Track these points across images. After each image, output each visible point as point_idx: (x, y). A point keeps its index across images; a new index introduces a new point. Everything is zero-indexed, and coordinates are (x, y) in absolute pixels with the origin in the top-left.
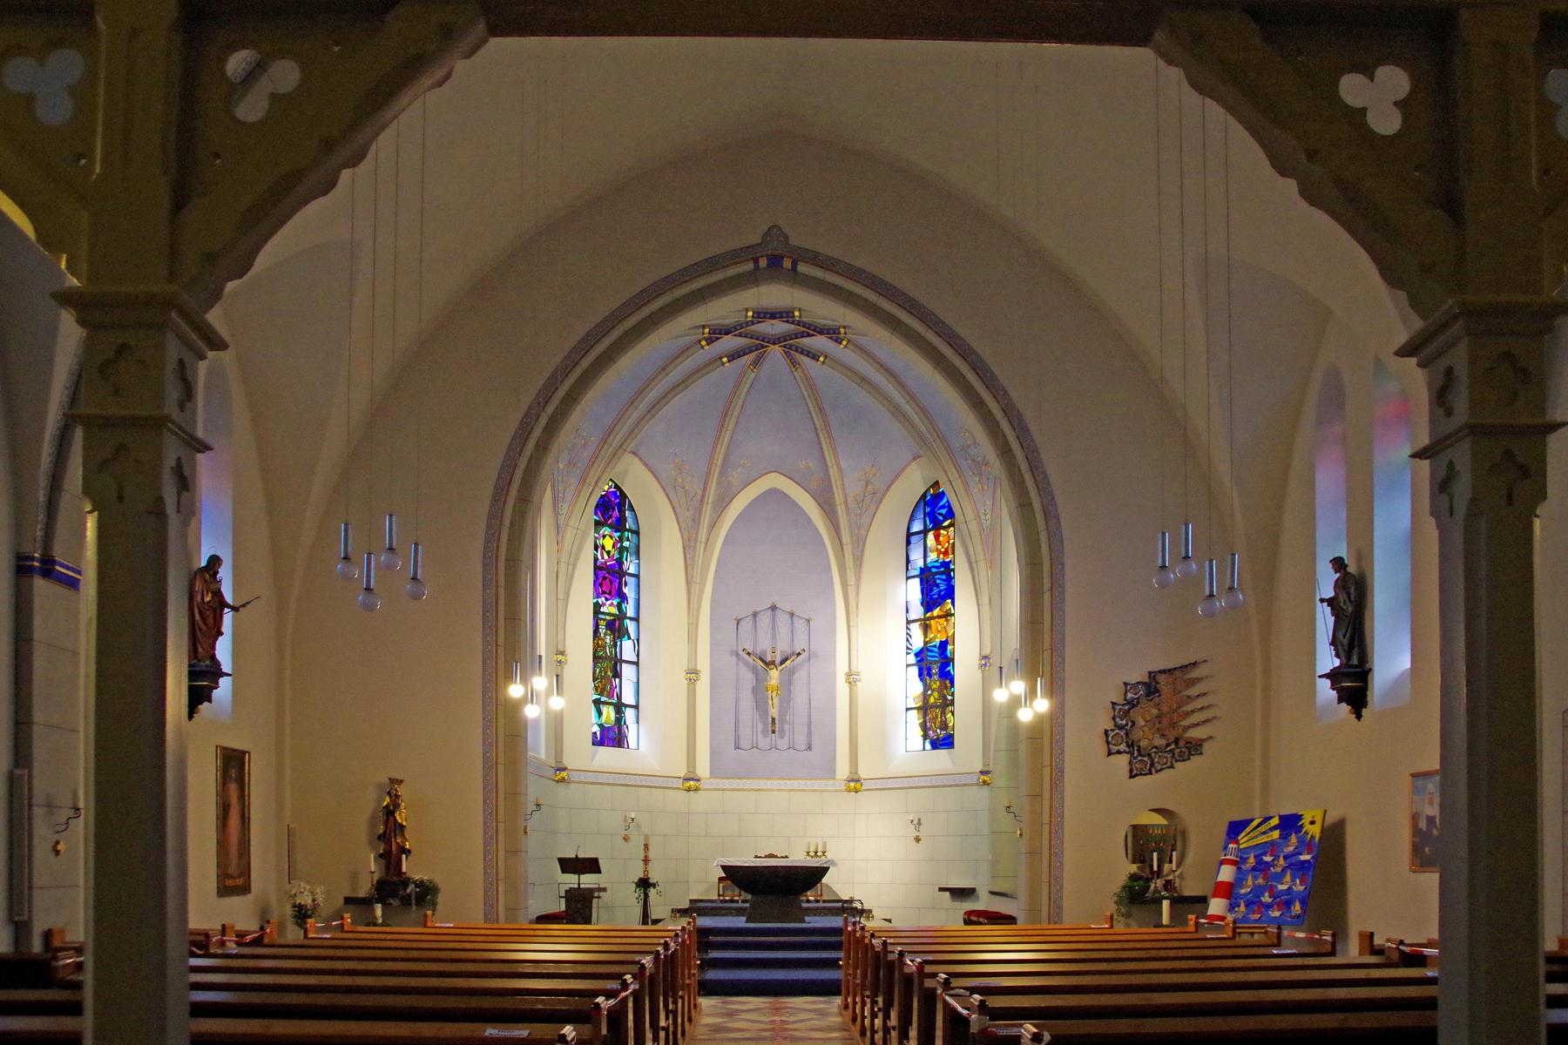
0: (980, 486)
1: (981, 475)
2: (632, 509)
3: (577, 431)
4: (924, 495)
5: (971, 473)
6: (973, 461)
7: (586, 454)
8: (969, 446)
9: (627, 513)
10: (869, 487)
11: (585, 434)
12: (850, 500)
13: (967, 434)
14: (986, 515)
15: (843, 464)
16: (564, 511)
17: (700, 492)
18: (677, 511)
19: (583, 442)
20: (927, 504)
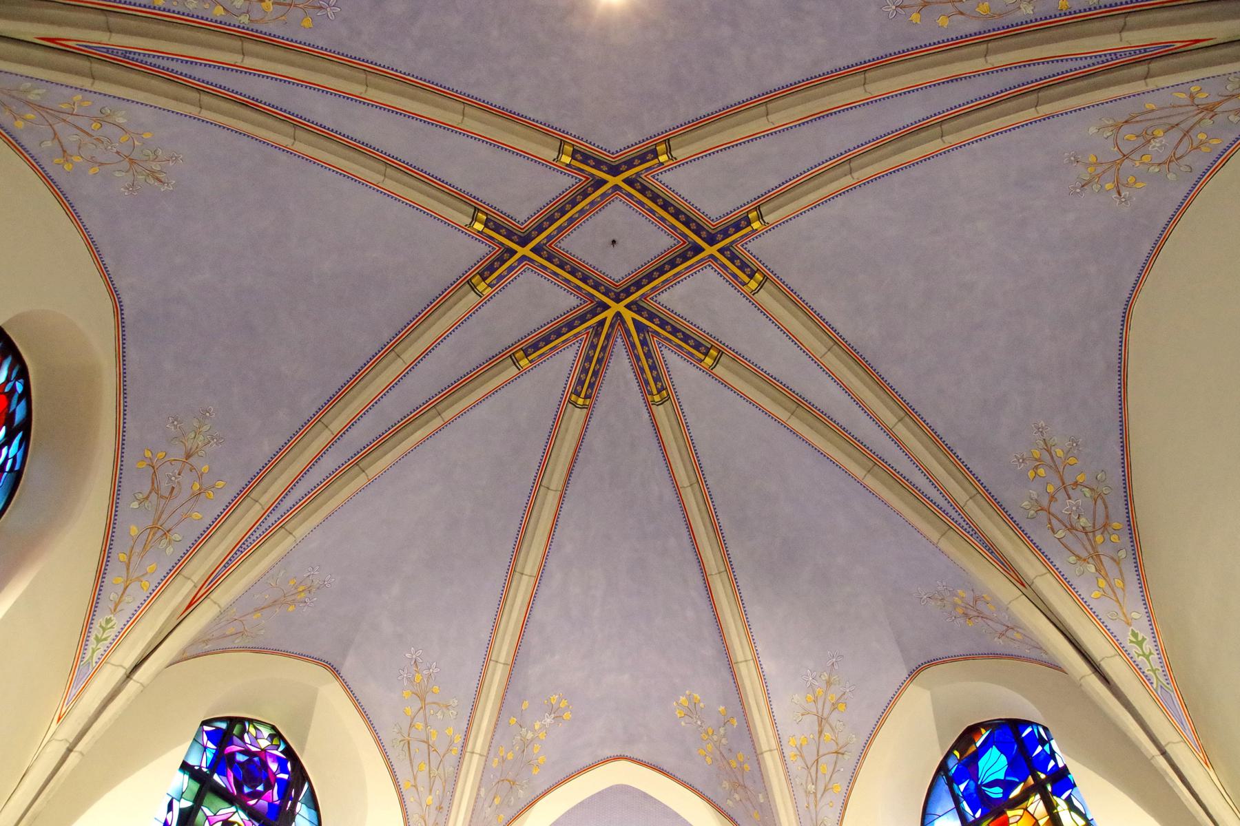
0: (1102, 583)
1: (1096, 557)
2: (314, 804)
3: (188, 456)
4: (943, 768)
5: (1073, 559)
6: (1071, 528)
7: (201, 517)
8: (1052, 498)
9: (301, 809)
10: (828, 735)
11: (205, 469)
12: (790, 753)
13: (1041, 471)
14: (1140, 644)
15: (769, 666)
16: (111, 634)
17: (458, 740)
18: (410, 799)
19: (197, 487)
20: (953, 781)
